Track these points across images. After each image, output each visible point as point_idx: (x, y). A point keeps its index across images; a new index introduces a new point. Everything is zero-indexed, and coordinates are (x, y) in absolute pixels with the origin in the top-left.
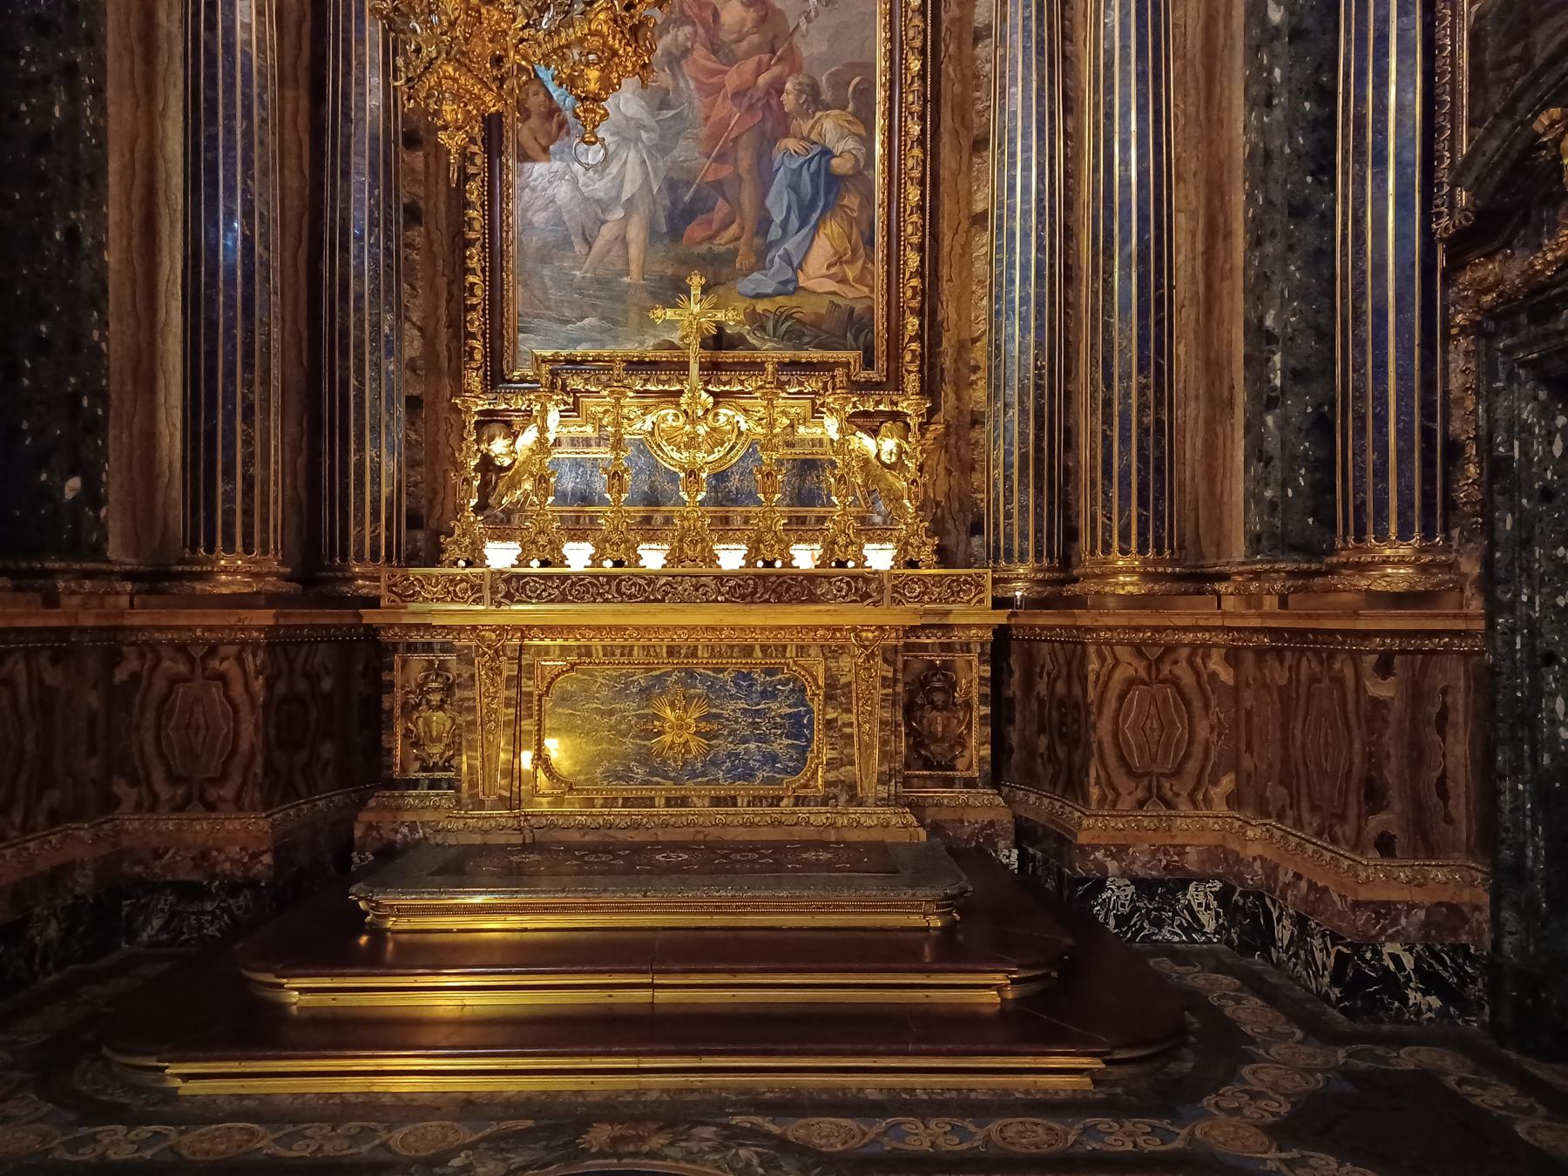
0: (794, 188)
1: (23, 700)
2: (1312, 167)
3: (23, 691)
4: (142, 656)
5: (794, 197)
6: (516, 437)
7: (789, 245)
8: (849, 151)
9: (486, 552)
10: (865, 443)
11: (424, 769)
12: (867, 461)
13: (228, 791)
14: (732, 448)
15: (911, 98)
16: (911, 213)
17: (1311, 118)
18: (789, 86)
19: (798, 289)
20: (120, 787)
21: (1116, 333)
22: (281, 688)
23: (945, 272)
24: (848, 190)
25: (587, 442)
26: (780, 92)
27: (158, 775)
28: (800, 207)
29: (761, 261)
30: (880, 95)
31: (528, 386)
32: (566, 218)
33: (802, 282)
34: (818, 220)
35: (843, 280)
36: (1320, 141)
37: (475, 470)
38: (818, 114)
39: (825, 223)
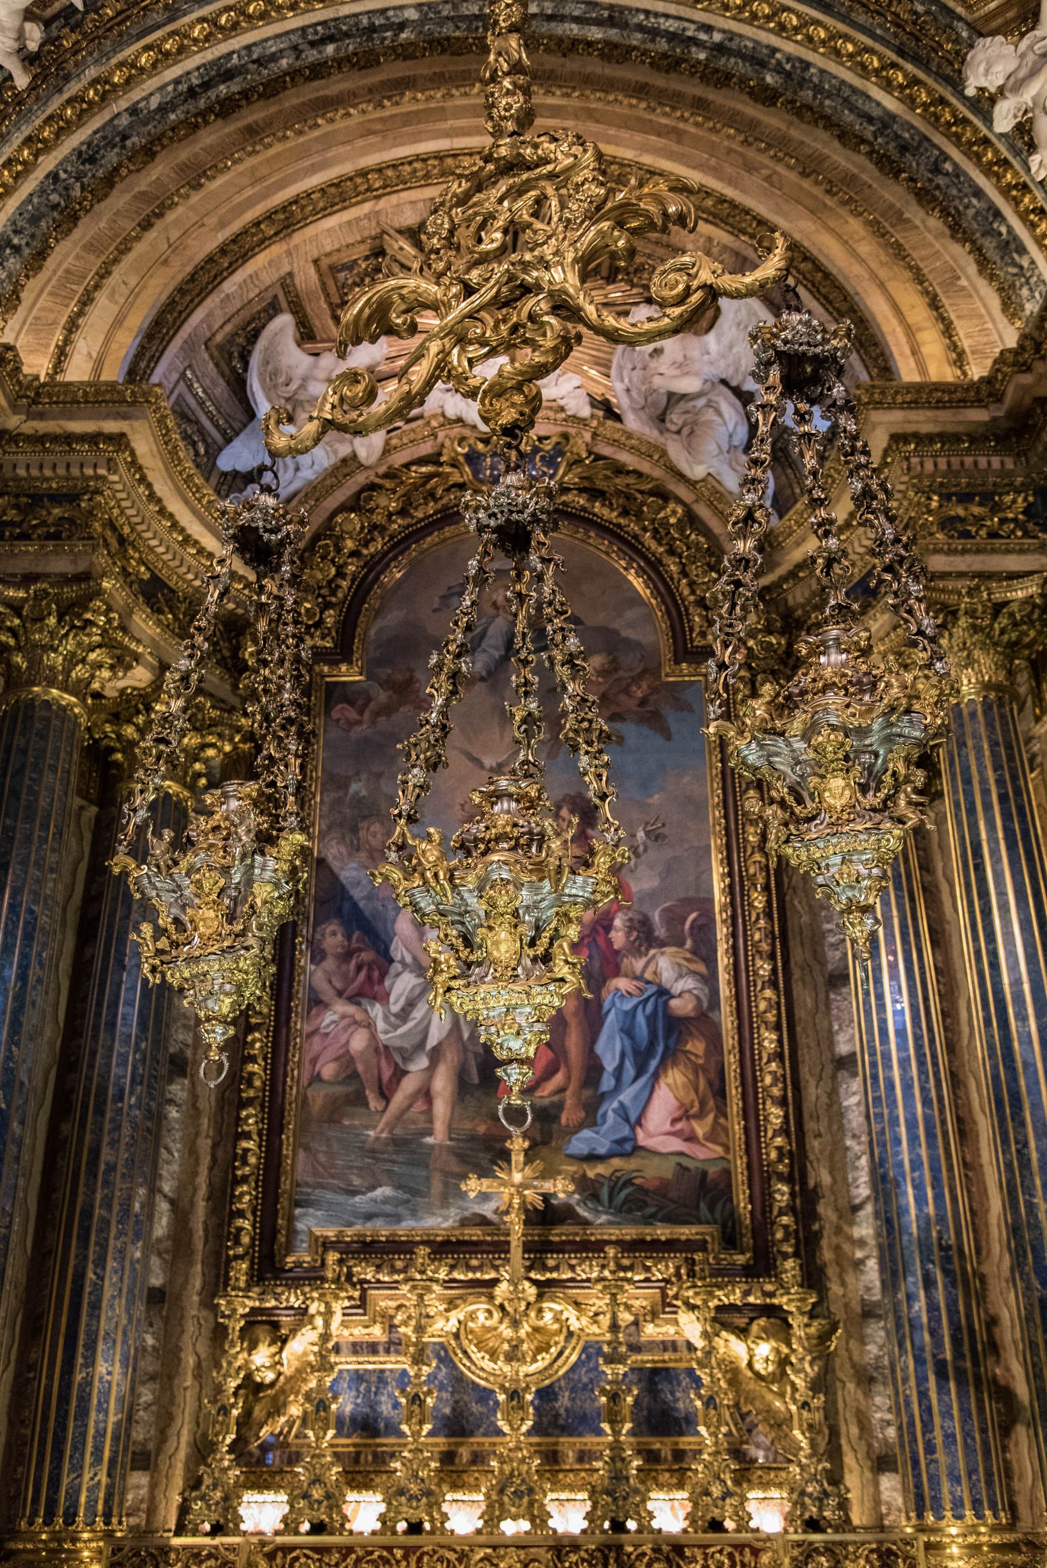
0: (628, 1031)
5: (627, 1043)
6: (284, 1341)
7: (626, 1096)
8: (689, 991)
9: (242, 1511)
10: (734, 1348)
14: (560, 1354)
15: (757, 937)
16: (769, 1062)
18: (618, 922)
19: (637, 1148)
23: (810, 1126)
24: (691, 1034)
25: (373, 1348)
26: (608, 928)
28: (636, 1052)
29: (591, 1116)
30: (722, 931)
31: (313, 1277)
32: (360, 1068)
34: (658, 1068)
37: (235, 1394)
38: (652, 952)
39: (665, 1071)
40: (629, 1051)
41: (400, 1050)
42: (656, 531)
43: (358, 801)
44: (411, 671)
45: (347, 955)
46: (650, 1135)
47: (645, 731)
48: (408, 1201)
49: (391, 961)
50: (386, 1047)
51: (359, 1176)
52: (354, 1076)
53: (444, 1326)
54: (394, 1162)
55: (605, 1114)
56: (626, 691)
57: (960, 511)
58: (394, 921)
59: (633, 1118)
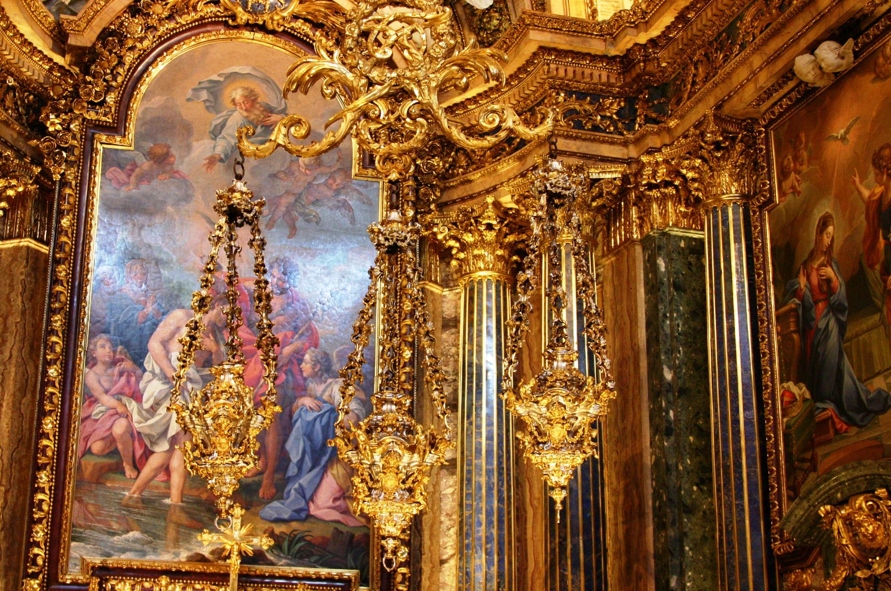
0: (309, 436)
2: (697, 480)
5: (308, 443)
7: (304, 480)
17: (694, 447)
18: (307, 357)
19: (309, 516)
21: (569, 583)
26: (300, 361)
28: (313, 451)
29: (279, 493)
32: (120, 447)
33: (313, 510)
34: (327, 462)
36: (701, 463)
40: (308, 449)
44: (169, 147)
45: (114, 363)
46: (318, 508)
48: (151, 542)
49: (145, 370)
50: (139, 433)
51: (117, 522)
52: (115, 452)
54: (142, 514)
55: (290, 491)
57: (578, 108)
58: (148, 342)
59: (308, 496)
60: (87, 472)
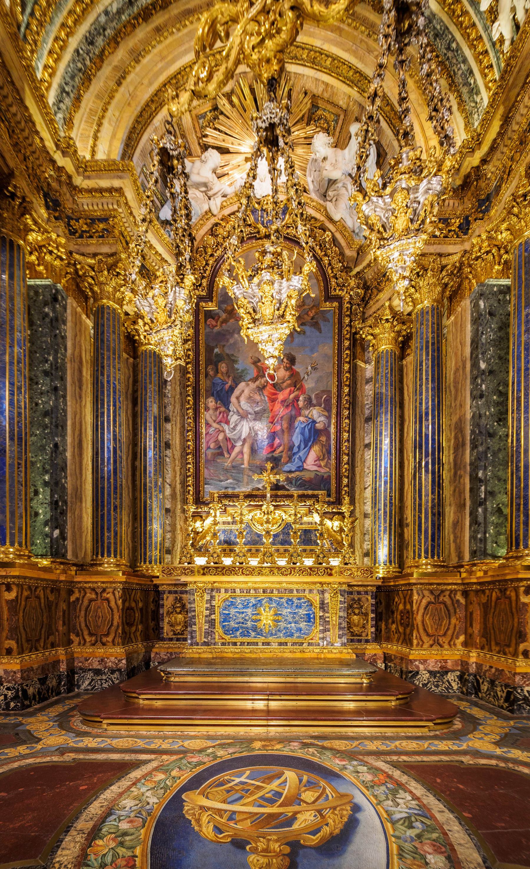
0: (302, 434)
1: (43, 605)
3: (42, 601)
4: (80, 592)
7: (301, 454)
10: (328, 523)
11: (175, 634)
12: (328, 530)
13: (110, 639)
18: (301, 398)
19: (304, 469)
20: (73, 637)
22: (127, 604)
25: (229, 523)
26: (298, 400)
27: (86, 633)
29: (290, 459)
33: (305, 466)
35: (320, 466)
41: (233, 439)
42: (321, 246)
43: (217, 355)
45: (216, 409)
47: (313, 329)
52: (220, 447)
53: (248, 517)
56: (307, 314)
60: (209, 457)
